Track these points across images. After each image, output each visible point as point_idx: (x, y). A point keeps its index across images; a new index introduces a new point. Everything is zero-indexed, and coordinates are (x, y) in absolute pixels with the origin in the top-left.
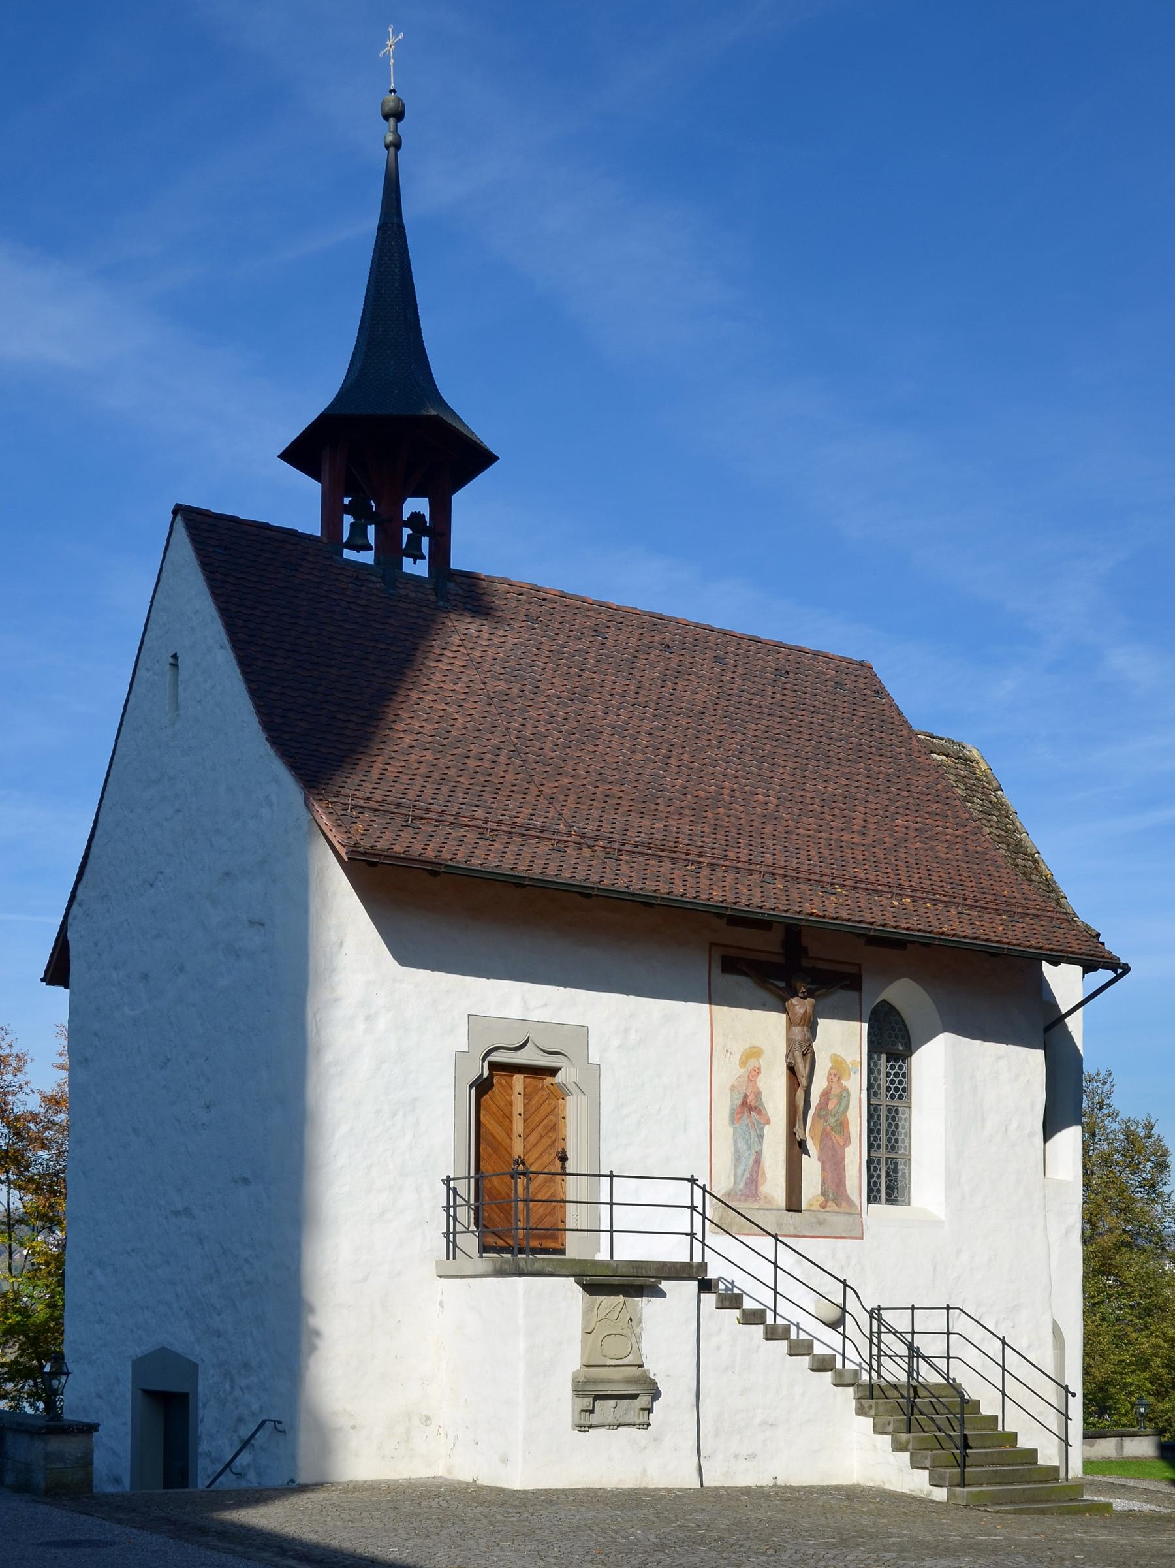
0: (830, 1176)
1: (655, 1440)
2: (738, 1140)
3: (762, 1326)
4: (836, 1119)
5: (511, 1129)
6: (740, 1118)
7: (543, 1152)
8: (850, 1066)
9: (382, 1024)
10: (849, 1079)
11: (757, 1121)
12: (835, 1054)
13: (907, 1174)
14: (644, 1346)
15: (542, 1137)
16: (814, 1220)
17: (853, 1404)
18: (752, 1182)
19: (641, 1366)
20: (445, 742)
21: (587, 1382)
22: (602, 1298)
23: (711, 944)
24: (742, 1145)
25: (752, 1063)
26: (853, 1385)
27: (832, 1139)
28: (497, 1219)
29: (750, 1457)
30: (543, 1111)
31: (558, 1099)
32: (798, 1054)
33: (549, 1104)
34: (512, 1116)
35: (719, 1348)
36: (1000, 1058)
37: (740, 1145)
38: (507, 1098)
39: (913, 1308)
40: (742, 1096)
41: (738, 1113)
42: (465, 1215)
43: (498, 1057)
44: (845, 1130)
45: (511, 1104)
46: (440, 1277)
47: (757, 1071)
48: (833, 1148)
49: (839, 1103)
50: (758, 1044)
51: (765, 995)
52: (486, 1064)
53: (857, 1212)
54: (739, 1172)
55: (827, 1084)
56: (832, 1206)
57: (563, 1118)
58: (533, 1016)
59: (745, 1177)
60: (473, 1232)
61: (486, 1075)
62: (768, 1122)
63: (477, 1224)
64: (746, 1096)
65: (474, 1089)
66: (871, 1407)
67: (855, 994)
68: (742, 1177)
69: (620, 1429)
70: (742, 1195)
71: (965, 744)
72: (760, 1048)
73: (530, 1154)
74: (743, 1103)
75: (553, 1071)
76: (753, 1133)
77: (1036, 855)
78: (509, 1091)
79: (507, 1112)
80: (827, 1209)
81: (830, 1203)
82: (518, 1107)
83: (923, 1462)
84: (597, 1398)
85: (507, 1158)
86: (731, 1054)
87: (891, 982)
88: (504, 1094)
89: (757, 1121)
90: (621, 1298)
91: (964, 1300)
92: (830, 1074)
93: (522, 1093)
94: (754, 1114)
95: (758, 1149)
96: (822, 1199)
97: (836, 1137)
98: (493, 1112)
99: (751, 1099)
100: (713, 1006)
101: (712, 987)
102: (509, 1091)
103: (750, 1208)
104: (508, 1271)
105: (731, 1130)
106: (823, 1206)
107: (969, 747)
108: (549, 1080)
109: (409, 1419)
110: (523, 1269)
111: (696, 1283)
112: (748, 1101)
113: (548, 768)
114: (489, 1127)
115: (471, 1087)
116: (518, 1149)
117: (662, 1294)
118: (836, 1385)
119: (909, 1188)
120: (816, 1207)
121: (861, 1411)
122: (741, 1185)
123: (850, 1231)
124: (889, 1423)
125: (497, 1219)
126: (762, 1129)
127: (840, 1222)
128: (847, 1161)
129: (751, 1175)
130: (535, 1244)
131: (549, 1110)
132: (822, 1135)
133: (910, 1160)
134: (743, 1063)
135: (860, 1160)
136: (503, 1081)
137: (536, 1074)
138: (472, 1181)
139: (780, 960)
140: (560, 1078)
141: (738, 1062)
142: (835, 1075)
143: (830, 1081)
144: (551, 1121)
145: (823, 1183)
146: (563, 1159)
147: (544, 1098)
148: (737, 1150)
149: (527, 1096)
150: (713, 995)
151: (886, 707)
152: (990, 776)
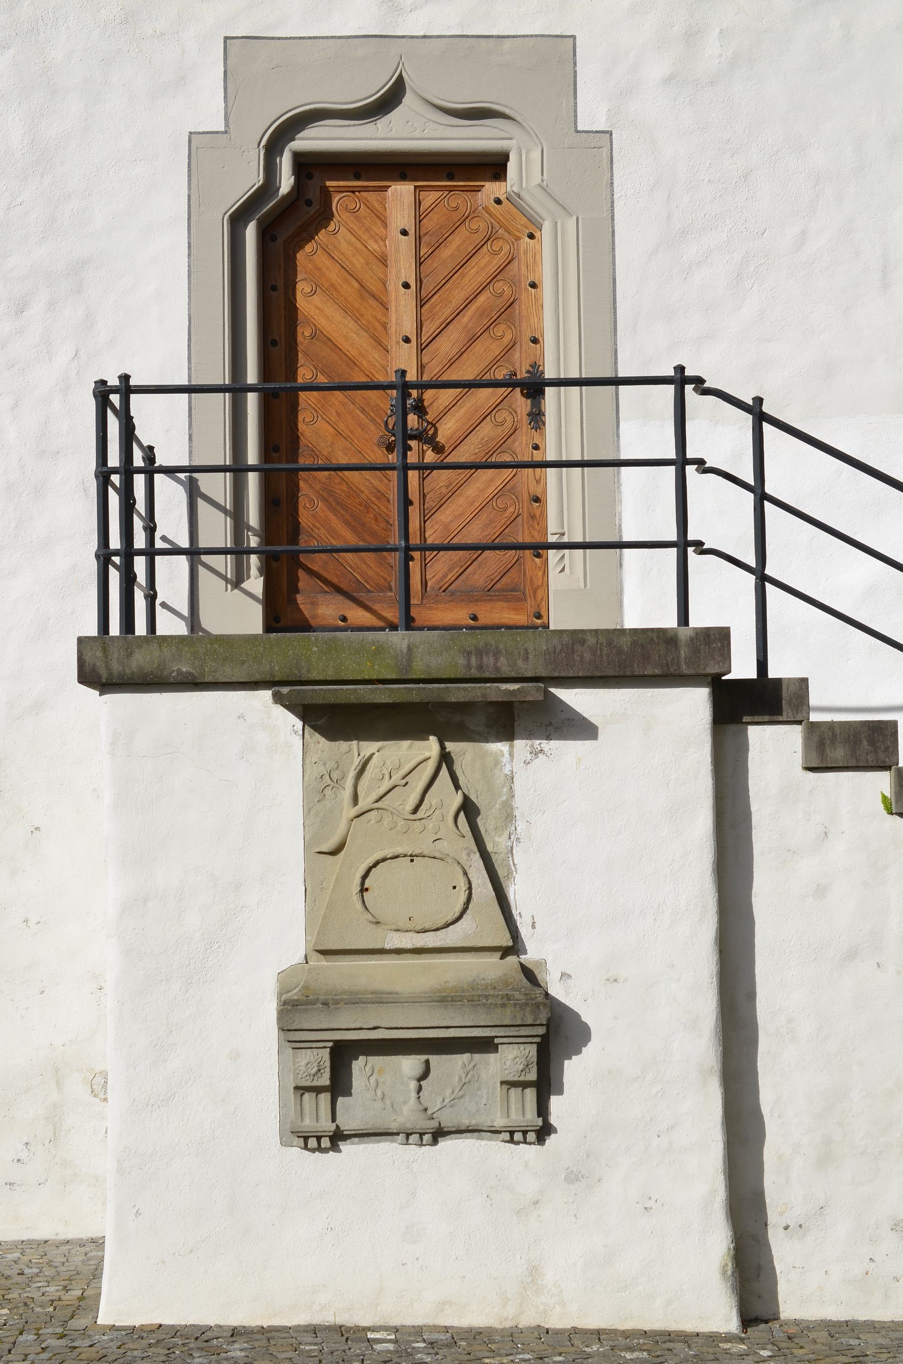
1: (573, 1178)
5: (385, 326)
15: (473, 339)
19: (515, 947)
22: (370, 747)
31: (518, 239)
35: (821, 891)
38: (372, 246)
45: (383, 261)
52: (285, 164)
57: (533, 285)
65: (251, 233)
78: (378, 229)
79: (374, 287)
88: (365, 237)
98: (333, 285)
108: (491, 189)
109: (59, 1085)
114: (322, 323)
115: (238, 220)
131: (492, 269)
137: (451, 178)
147: (478, 238)
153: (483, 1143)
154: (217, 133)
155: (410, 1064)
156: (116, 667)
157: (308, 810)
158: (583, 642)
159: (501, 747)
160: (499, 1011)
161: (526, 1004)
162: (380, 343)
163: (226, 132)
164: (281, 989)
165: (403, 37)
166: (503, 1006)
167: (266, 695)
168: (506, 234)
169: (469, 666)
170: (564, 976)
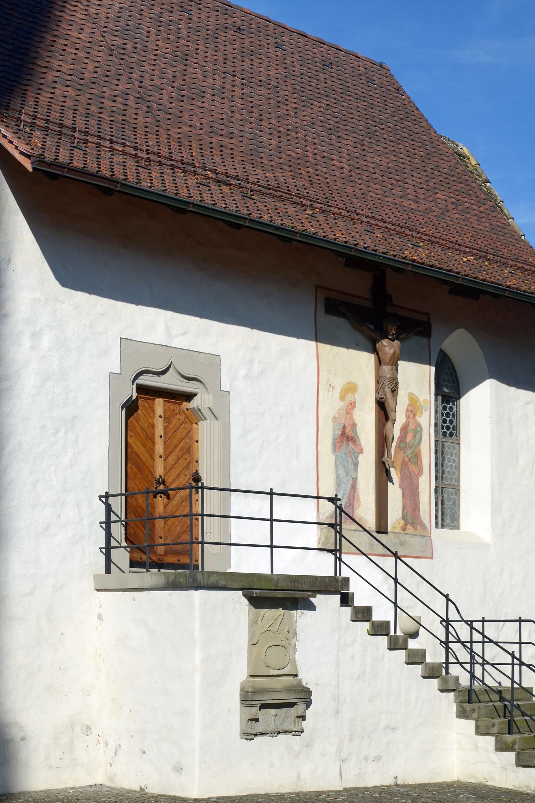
0: (408, 502)
2: (339, 467)
3: (386, 637)
4: (412, 451)
5: (153, 450)
6: (340, 447)
7: (180, 473)
8: (422, 404)
9: (46, 341)
11: (353, 450)
13: (457, 503)
14: (300, 657)
15: (179, 459)
16: (397, 541)
17: (454, 707)
18: (350, 505)
20: (82, 82)
21: (256, 692)
23: (317, 287)
24: (341, 471)
25: (349, 397)
26: (453, 690)
27: (408, 469)
28: (142, 535)
29: (377, 759)
30: (180, 434)
31: (192, 424)
32: (388, 390)
33: (185, 428)
34: (154, 438)
36: (528, 403)
38: (150, 420)
39: (520, 620)
40: (341, 427)
41: (338, 443)
42: (118, 530)
43: (146, 380)
45: (153, 426)
46: (98, 590)
48: (410, 477)
49: (415, 436)
50: (354, 381)
51: (358, 336)
52: (135, 386)
56: (410, 528)
58: (176, 343)
60: (125, 547)
61: (134, 397)
62: (361, 452)
63: (126, 539)
64: (344, 427)
66: (473, 711)
67: (425, 340)
69: (280, 736)
71: (457, 142)
72: (356, 385)
73: (169, 474)
74: (342, 433)
75: (189, 397)
76: (350, 461)
77: (523, 237)
78: (151, 414)
80: (407, 532)
81: (409, 526)
82: (159, 430)
83: (531, 761)
84: (263, 707)
85: (150, 477)
87: (457, 329)
88: (148, 417)
89: (353, 450)
90: (281, 611)
91: (506, 613)
92: (407, 410)
93: (163, 417)
94: (351, 444)
95: (354, 476)
96: (402, 522)
97: (412, 468)
98: (138, 433)
99: (348, 429)
100: (319, 344)
101: (318, 326)
102: (151, 414)
103: (348, 530)
104: (184, 584)
105: (333, 458)
106: (404, 529)
107: (460, 145)
109: (73, 730)
110: (200, 582)
111: (339, 596)
112: (347, 432)
113: (170, 116)
114: (135, 447)
115: (123, 407)
116: (159, 470)
117: (312, 607)
118: (441, 691)
119: (459, 514)
120: (398, 530)
121: (462, 714)
124: (493, 725)
125: (142, 535)
126: (357, 458)
127: (415, 542)
128: (421, 488)
129: (349, 499)
130: (172, 559)
131: (184, 433)
132: (402, 465)
133: (459, 490)
134: (342, 397)
135: (430, 488)
136: (146, 404)
137: (174, 398)
138: (123, 497)
139: (369, 305)
140: (194, 403)
141: (338, 396)
143: (408, 417)
144: (186, 444)
145: (404, 508)
146: (197, 479)
147: (180, 422)
148: (338, 477)
149: (167, 419)
150: (318, 334)
151: (406, 102)
152: (479, 170)
153: (287, 736)
154: (118, 374)
155: (273, 711)
156: (206, 581)
157: (249, 629)
158: (317, 580)
159: (295, 612)
160: (301, 694)
161: (307, 692)
162: (152, 457)
163: (121, 374)
164: (241, 688)
165: (173, 347)
166: (302, 692)
167: (240, 593)
168: (188, 422)
169: (291, 586)
170: (307, 684)
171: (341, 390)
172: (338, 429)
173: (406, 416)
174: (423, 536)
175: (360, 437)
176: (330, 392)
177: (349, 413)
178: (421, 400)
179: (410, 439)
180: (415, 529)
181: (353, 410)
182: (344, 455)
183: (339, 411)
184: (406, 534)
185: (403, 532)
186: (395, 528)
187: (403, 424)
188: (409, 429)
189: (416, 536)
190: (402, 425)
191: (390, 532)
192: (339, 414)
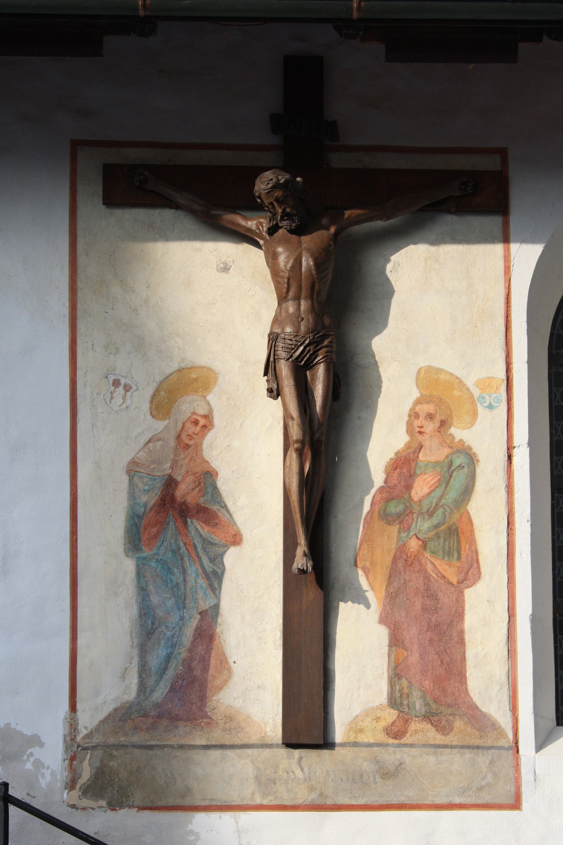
0: (414, 658)
2: (151, 587)
4: (435, 520)
6: (155, 537)
8: (476, 392)
10: (472, 423)
11: (204, 540)
12: (429, 369)
37: (155, 599)
40: (159, 485)
44: (465, 547)
47: (202, 422)
53: (502, 743)
54: (154, 662)
55: (406, 438)
59: (171, 673)
68: (164, 670)
70: (160, 716)
80: (403, 741)
81: (415, 726)
86: (127, 388)
92: (414, 415)
95: (204, 605)
96: (391, 715)
105: (130, 565)
112: (179, 493)
122: (159, 695)
123: (480, 789)
132: (395, 560)
141: (146, 406)
142: (430, 417)
171: (157, 391)
172: (148, 491)
173: (410, 430)
174: (478, 747)
175: (229, 504)
176: (118, 400)
177: (187, 446)
178: (470, 383)
179: (426, 490)
180: (444, 730)
181: (204, 436)
182: (170, 555)
183: (151, 445)
184: (406, 745)
185: (391, 741)
186: (361, 731)
187: (396, 454)
188: (421, 464)
189: (448, 751)
190: (392, 455)
191: (343, 745)
192: (150, 451)
